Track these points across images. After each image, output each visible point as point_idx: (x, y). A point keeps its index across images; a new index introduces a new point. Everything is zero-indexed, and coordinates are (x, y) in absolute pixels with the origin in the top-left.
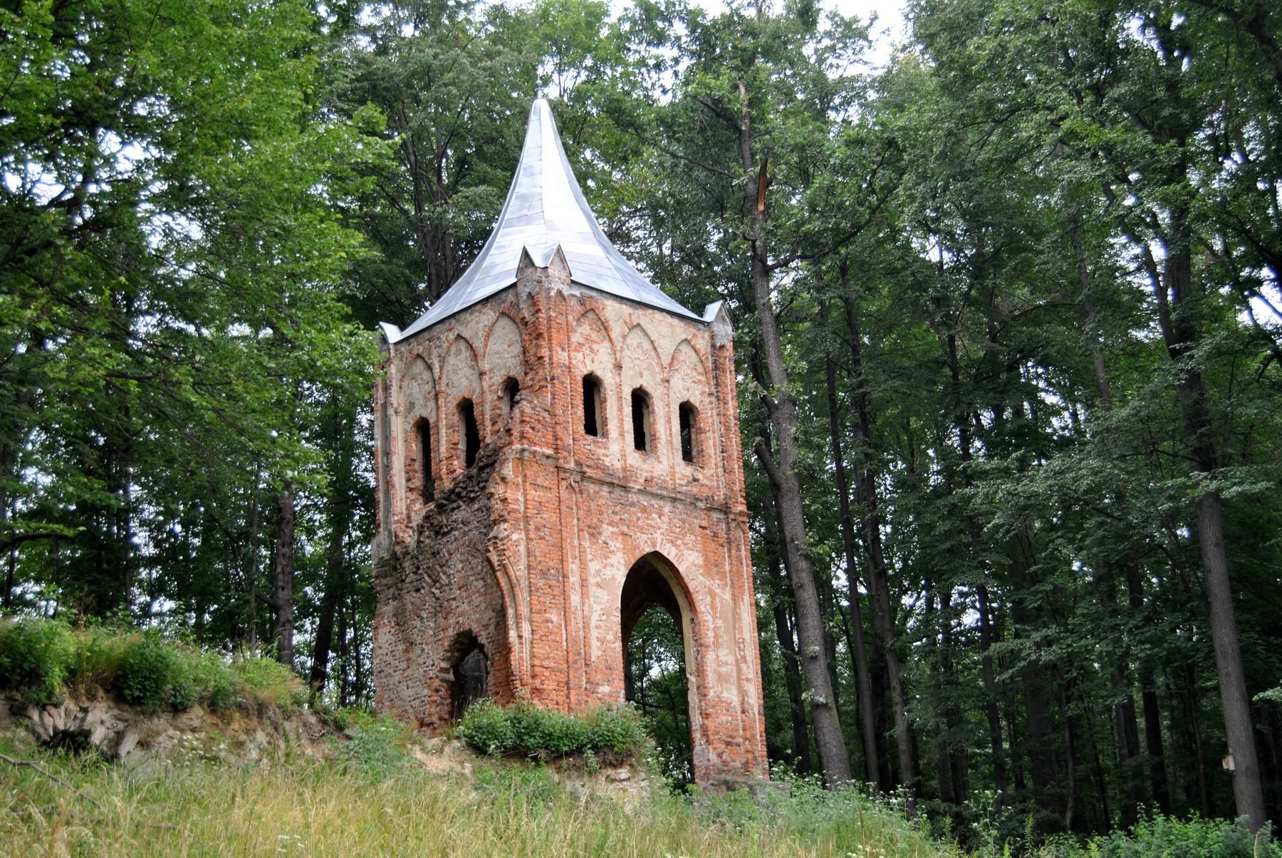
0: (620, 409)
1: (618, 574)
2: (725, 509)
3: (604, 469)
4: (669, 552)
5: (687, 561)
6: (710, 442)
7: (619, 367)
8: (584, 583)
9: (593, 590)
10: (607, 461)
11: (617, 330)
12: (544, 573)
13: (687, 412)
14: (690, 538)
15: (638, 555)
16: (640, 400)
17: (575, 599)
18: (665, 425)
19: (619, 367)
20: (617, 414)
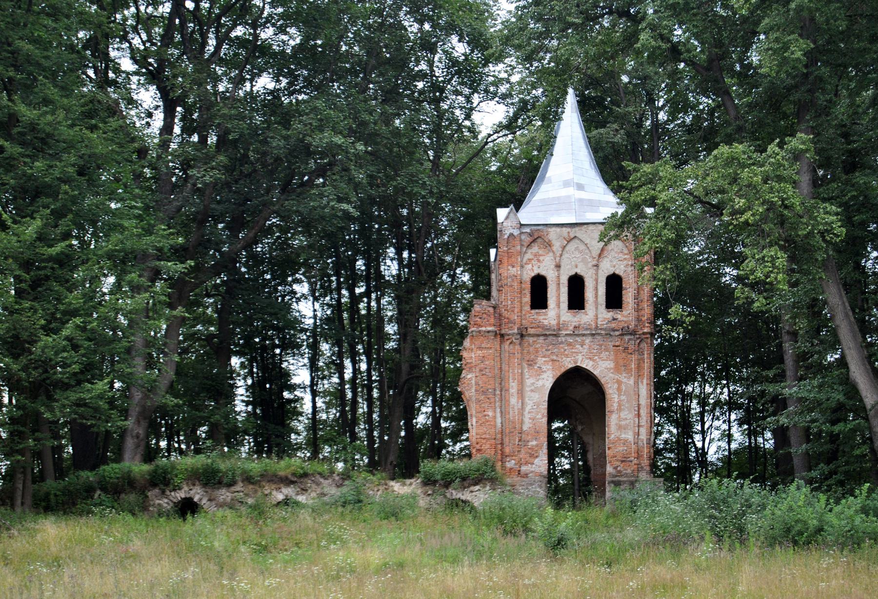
1: (548, 381)
2: (633, 333)
3: (543, 327)
4: (587, 365)
5: (601, 367)
6: (628, 296)
7: (558, 266)
8: (521, 393)
9: (528, 393)
10: (546, 322)
11: (557, 246)
12: (484, 393)
13: (614, 284)
14: (604, 355)
15: (563, 370)
16: (576, 285)
17: (513, 401)
19: (558, 266)
20: (557, 295)
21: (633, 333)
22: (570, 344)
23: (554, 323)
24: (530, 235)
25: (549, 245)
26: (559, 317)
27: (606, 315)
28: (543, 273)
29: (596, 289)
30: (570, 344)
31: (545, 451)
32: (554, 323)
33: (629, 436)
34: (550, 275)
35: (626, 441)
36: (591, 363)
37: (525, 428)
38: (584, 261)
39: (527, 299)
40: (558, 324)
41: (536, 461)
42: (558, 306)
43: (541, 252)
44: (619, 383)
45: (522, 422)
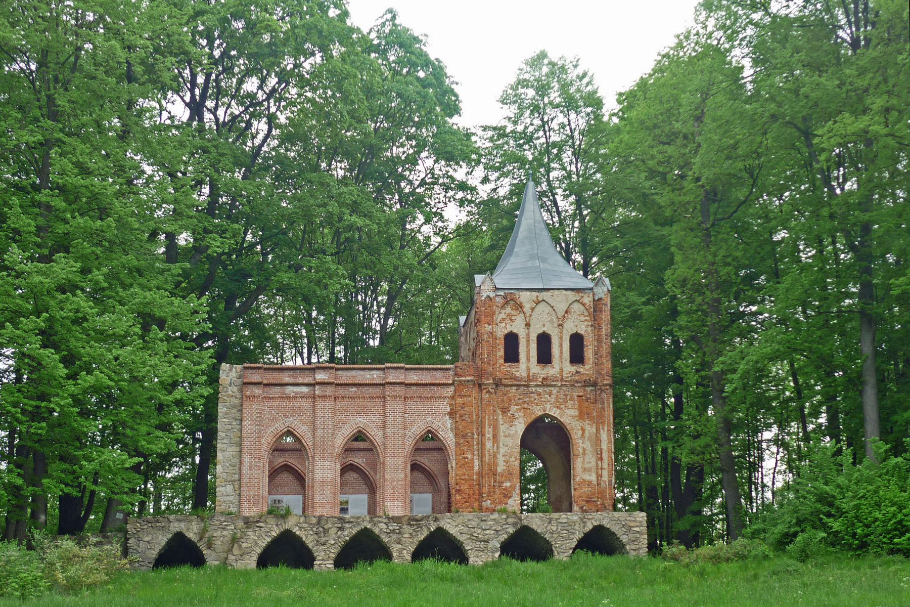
1: (520, 428)
2: (595, 384)
3: (516, 379)
4: (555, 412)
5: (568, 416)
6: (589, 353)
7: (528, 325)
8: (495, 436)
9: (502, 439)
10: (518, 374)
11: (527, 307)
12: (464, 436)
13: (577, 341)
14: (570, 403)
15: (533, 417)
16: (544, 341)
17: (489, 445)
18: (561, 349)
19: (528, 325)
20: (528, 350)
21: (595, 384)
22: (539, 394)
23: (525, 374)
24: (505, 297)
25: (519, 307)
26: (528, 370)
27: (569, 368)
33: (593, 478)
35: (590, 483)
37: (499, 470)
38: (551, 322)
39: (501, 353)
41: (510, 501)
45: (496, 464)
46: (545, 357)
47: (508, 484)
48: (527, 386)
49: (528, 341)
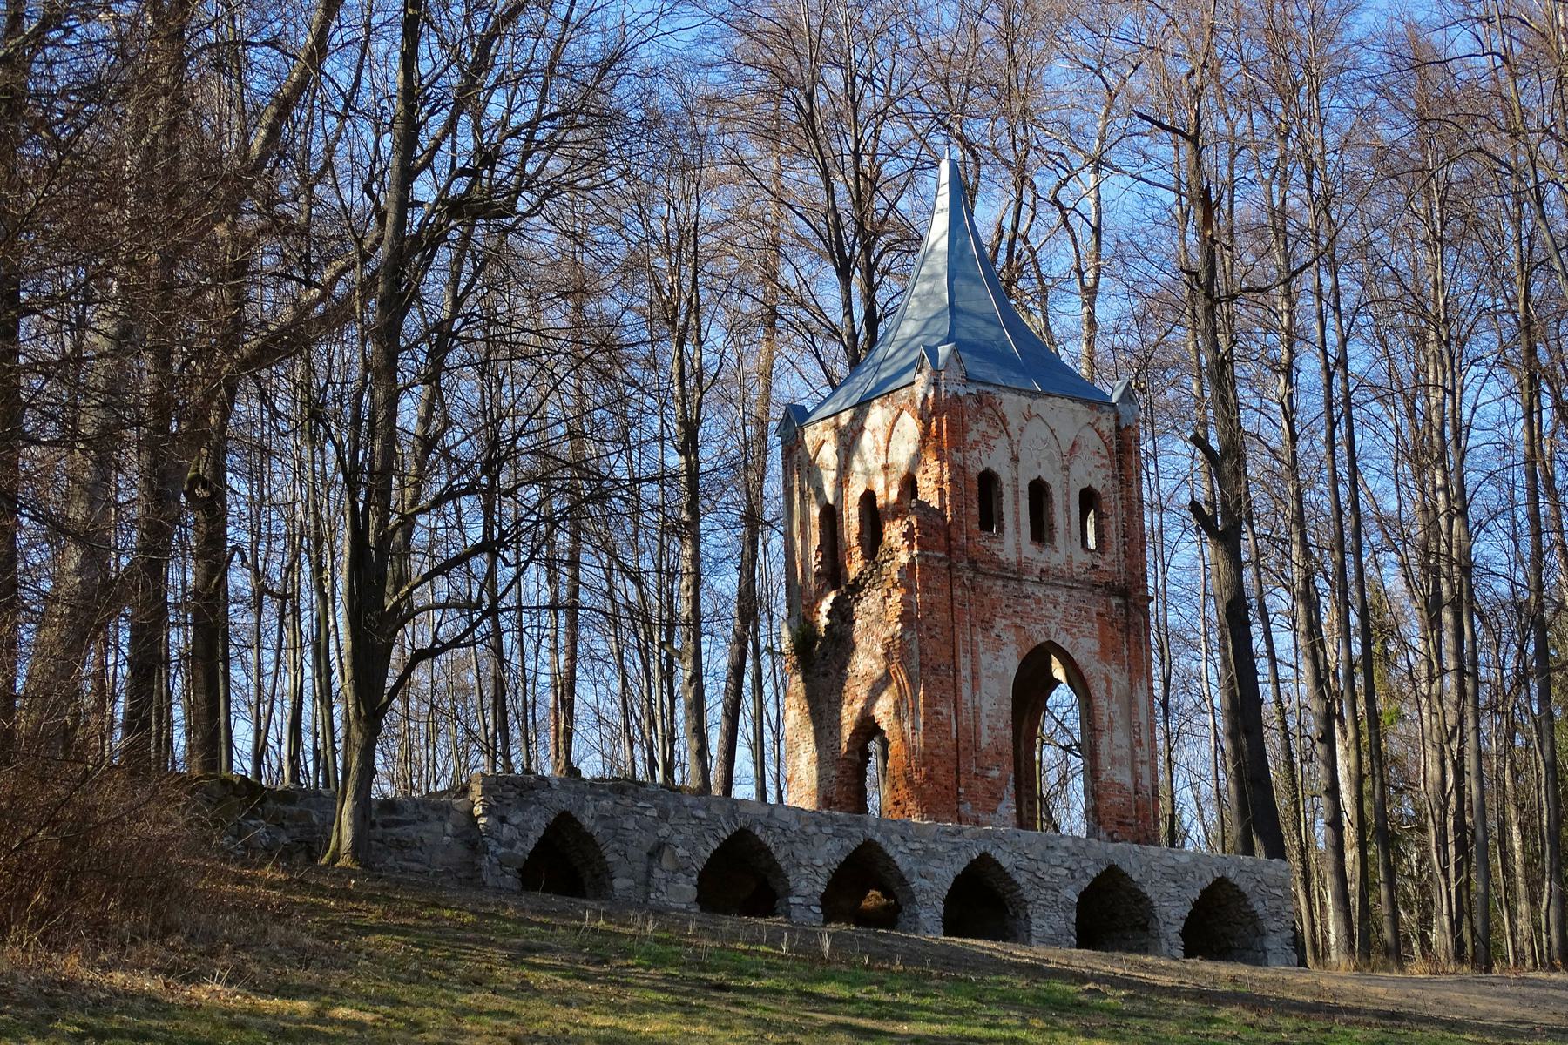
0: (1016, 503)
7: (1015, 459)
8: (975, 677)
9: (984, 682)
11: (1014, 423)
14: (1086, 626)
15: (1031, 645)
16: (1039, 492)
17: (966, 691)
19: (1015, 459)
20: (1015, 510)
22: (1038, 602)
26: (1019, 550)
28: (995, 469)
29: (1067, 510)
30: (1038, 602)
31: (1012, 790)
32: (1013, 558)
34: (1005, 475)
36: (1069, 639)
37: (985, 740)
38: (1050, 458)
39: (975, 511)
40: (1019, 563)
42: (1018, 528)
43: (991, 432)
44: (1108, 681)
45: (977, 733)
46: (1041, 530)
47: (995, 773)
48: (1019, 580)
49: (1016, 492)
